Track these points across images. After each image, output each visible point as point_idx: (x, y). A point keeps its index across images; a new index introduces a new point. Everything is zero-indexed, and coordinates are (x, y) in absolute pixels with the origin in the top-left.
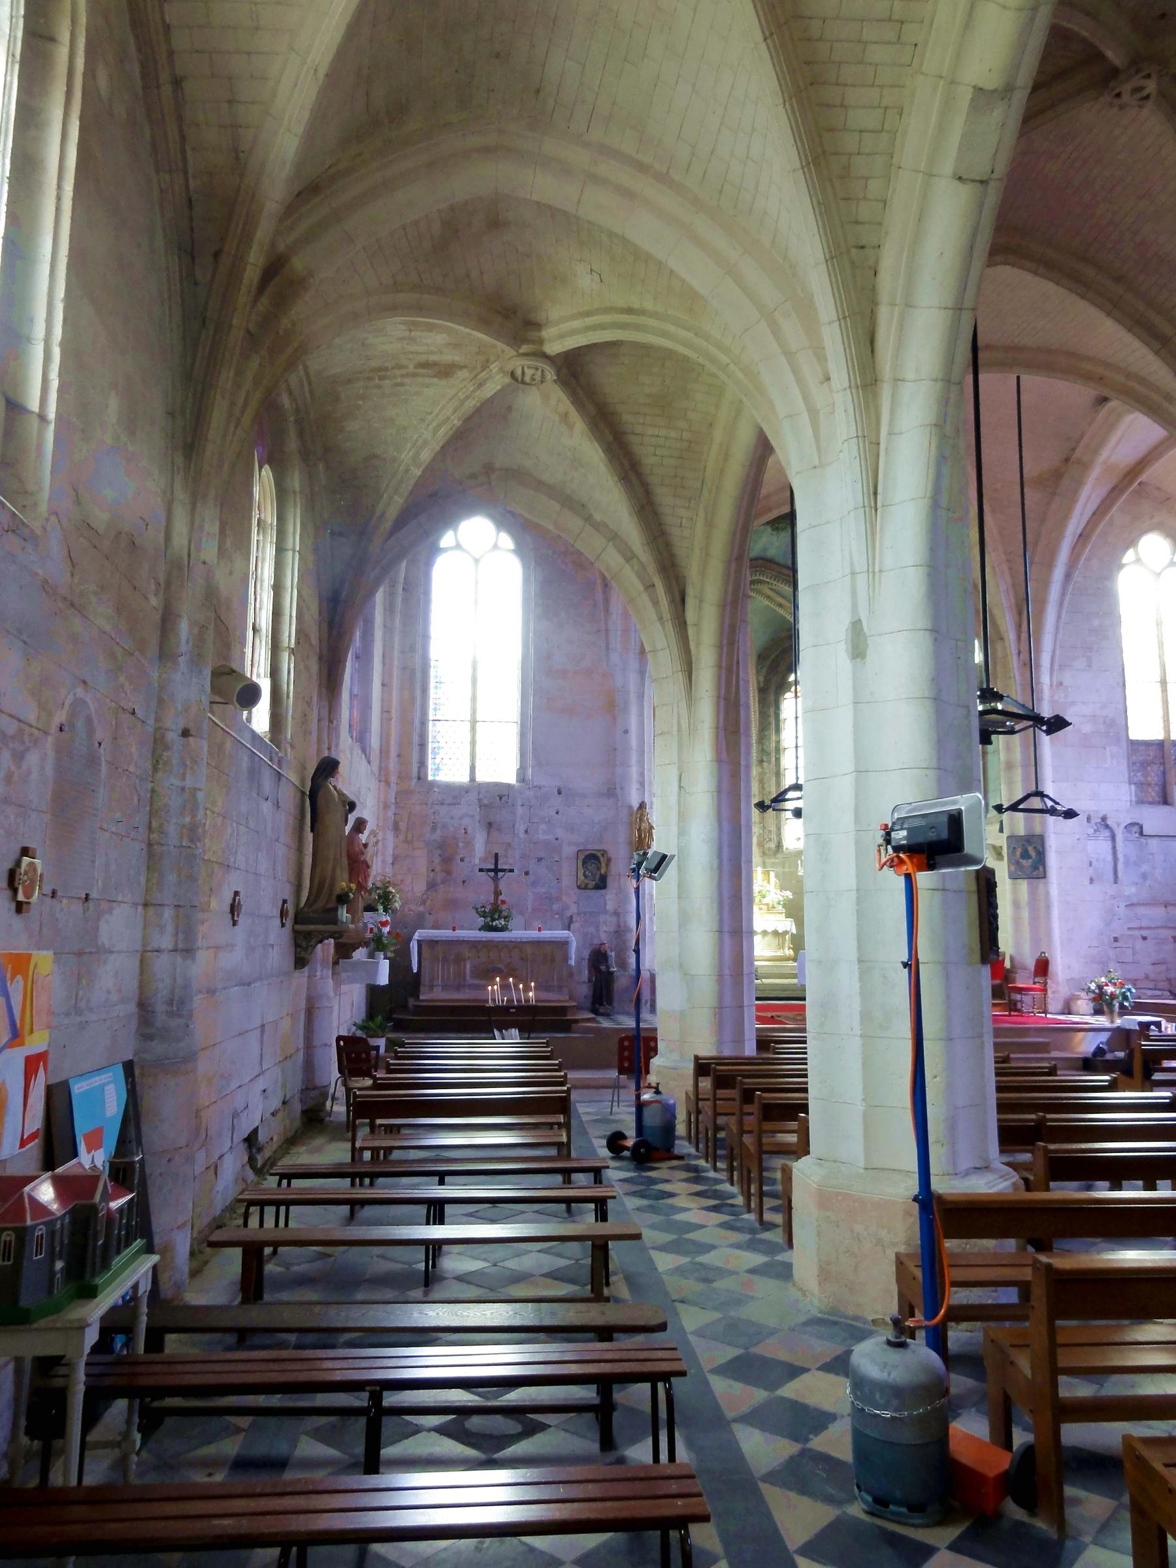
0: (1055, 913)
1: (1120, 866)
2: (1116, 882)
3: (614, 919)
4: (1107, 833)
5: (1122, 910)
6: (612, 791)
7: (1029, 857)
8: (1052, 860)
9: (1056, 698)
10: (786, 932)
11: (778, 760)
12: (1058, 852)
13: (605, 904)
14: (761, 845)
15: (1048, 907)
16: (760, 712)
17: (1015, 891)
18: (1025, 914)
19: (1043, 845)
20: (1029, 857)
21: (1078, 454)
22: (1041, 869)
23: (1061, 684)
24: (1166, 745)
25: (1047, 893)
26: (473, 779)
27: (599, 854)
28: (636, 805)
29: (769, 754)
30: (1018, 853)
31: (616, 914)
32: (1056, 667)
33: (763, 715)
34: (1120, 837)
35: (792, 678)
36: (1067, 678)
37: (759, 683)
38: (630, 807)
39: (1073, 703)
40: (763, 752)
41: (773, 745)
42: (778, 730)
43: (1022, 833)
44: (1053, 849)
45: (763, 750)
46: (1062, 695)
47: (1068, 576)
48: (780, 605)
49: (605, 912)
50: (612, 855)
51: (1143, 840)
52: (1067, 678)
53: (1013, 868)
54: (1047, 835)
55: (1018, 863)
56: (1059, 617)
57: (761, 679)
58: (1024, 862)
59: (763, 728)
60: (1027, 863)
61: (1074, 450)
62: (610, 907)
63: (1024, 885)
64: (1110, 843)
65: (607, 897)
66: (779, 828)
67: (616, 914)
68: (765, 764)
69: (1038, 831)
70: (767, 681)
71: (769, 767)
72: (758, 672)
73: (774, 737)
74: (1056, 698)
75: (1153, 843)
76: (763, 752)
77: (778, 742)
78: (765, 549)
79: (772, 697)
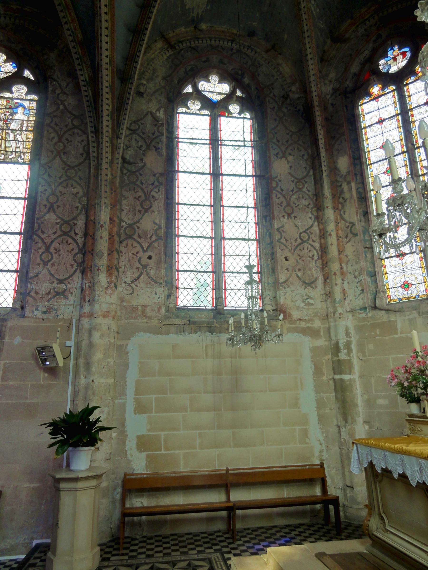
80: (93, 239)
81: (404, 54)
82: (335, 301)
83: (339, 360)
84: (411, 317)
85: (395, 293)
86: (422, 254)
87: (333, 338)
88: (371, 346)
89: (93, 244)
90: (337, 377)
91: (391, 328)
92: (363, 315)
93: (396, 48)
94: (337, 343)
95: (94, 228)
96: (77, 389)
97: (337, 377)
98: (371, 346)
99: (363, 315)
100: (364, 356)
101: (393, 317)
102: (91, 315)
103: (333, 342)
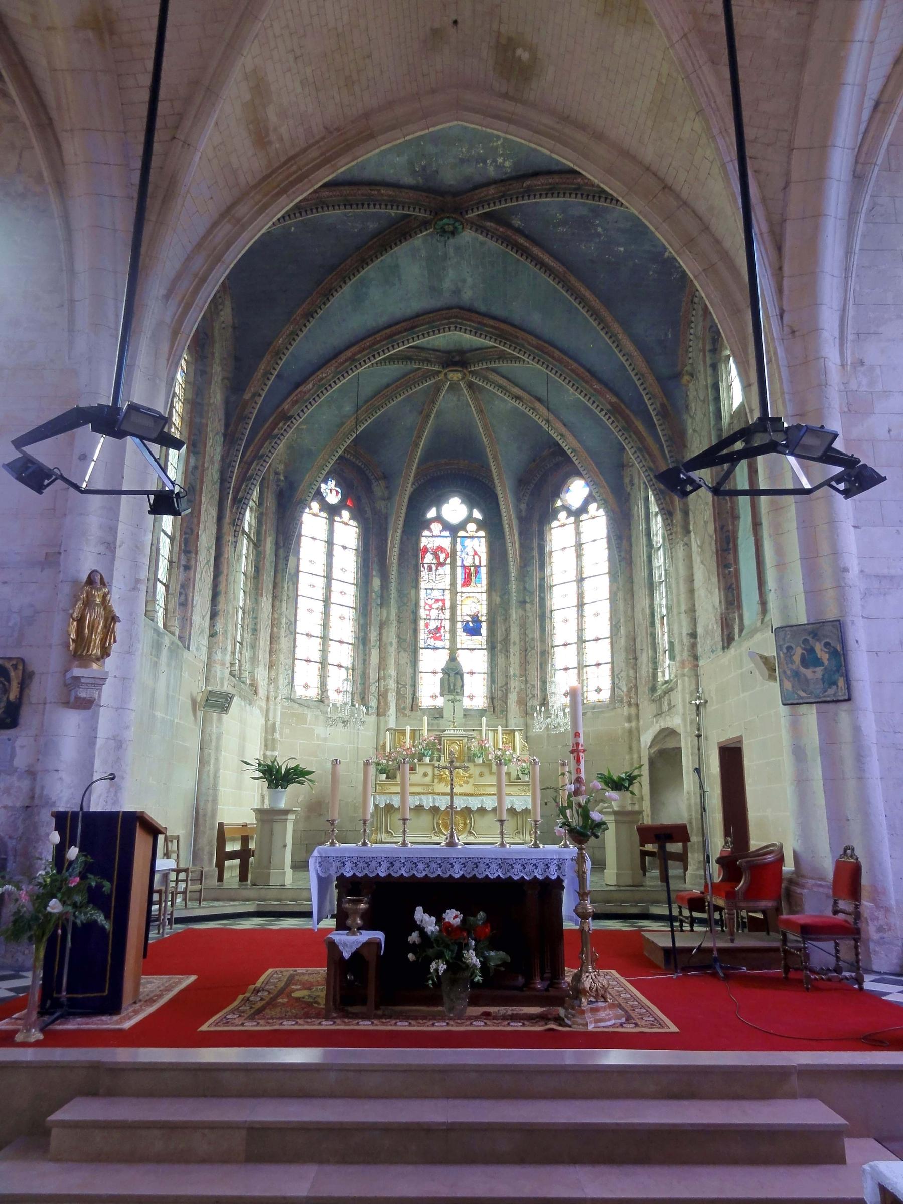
0: (874, 766)
3: (25, 784)
6: (52, 557)
7: (817, 662)
8: (862, 666)
9: (853, 386)
10: (526, 811)
11: (542, 600)
12: (874, 653)
13: (13, 756)
14: (522, 702)
15: (860, 758)
16: (522, 546)
18: (817, 772)
19: (843, 641)
20: (817, 662)
22: (841, 682)
23: (862, 363)
25: (857, 730)
26: (347, 669)
27: (8, 665)
28: (84, 578)
29: (532, 594)
30: (797, 658)
31: (31, 774)
32: (850, 337)
33: (525, 548)
35: (559, 503)
36: (872, 352)
37: (519, 512)
38: (75, 582)
39: (887, 394)
40: (524, 590)
41: (537, 582)
42: (542, 567)
43: (803, 620)
44: (863, 646)
45: (525, 589)
46: (864, 381)
47: (858, 178)
48: (517, 398)
49: (11, 770)
50: (35, 665)
52: (872, 352)
53: (788, 685)
54: (849, 619)
56: (848, 252)
57: (523, 506)
58: (808, 673)
59: (525, 564)
60: (813, 674)
62: (21, 760)
63: (810, 716)
65: (18, 743)
66: (544, 682)
67: (31, 774)
68: (528, 606)
69: (831, 613)
70: (530, 508)
71: (532, 609)
72: (518, 500)
73: (537, 574)
74: (853, 386)
76: (524, 590)
77: (543, 579)
78: (457, 292)
79: (535, 527)
80: (227, 580)
81: (337, 491)
82: (278, 688)
83: (273, 739)
84: (317, 714)
85: (300, 692)
86: (320, 665)
87: (271, 719)
88: (287, 731)
89: (227, 586)
90: (269, 753)
91: (302, 719)
92: (286, 704)
93: (333, 482)
94: (274, 724)
95: (228, 568)
96: (207, 738)
97: (269, 753)
98: (287, 731)
99: (286, 704)
100: (282, 738)
101: (306, 711)
102: (223, 664)
103: (270, 723)
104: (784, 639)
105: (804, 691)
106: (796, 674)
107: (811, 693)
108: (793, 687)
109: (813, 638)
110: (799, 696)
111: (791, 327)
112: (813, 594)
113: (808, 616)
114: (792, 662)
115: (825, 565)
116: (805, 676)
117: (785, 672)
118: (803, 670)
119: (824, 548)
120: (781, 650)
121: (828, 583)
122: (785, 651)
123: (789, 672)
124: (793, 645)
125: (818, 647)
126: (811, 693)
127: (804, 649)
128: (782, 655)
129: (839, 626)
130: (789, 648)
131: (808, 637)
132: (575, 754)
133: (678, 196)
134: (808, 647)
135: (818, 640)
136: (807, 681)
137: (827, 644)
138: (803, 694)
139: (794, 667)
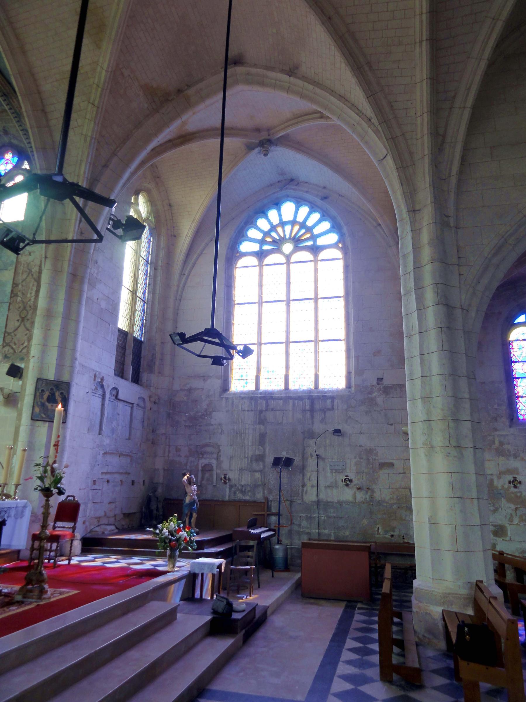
1: (105, 420)
2: (100, 434)
4: (100, 392)
5: (100, 457)
17: (32, 433)
19: (68, 392)
21: (190, 92)
24: (129, 336)
34: (108, 396)
43: (51, 376)
51: (117, 402)
53: (37, 410)
55: (43, 405)
61: (189, 86)
64: (101, 399)
69: (65, 379)
75: (121, 405)
104: (41, 385)
105: (45, 414)
106: (43, 405)
107: (48, 416)
108: (40, 411)
109: (56, 388)
110: (41, 416)
111: (81, 230)
112: (60, 366)
113: (55, 376)
114: (42, 398)
115: (69, 353)
116: (47, 407)
117: (37, 402)
118: (47, 403)
119: (70, 345)
120: (38, 390)
121: (68, 363)
122: (40, 391)
123: (39, 403)
124: (45, 390)
125: (57, 394)
126: (48, 416)
127: (50, 393)
128: (38, 394)
129: (68, 385)
130: (43, 391)
131: (54, 388)
132: (56, 447)
133: (47, 121)
134: (52, 392)
135: (58, 390)
136: (48, 409)
137: (62, 393)
138: (44, 416)
139: (43, 401)
